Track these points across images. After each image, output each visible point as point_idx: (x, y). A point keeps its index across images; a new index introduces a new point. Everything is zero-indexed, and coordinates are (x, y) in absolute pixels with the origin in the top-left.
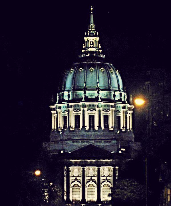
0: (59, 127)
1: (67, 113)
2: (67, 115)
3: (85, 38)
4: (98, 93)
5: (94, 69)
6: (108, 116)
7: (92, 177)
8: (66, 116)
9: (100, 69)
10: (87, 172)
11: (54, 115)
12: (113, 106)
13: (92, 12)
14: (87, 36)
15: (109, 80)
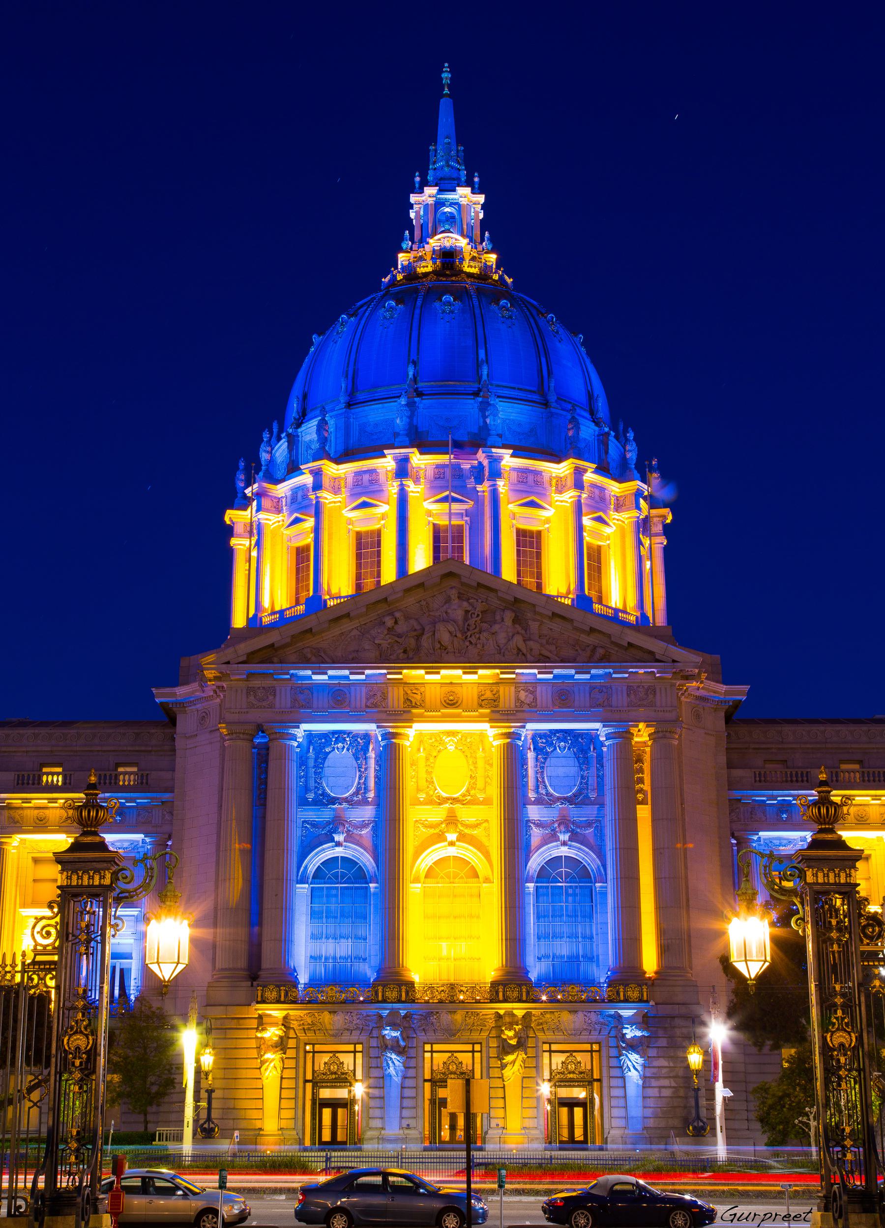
0: (266, 603)
1: (310, 522)
2: (309, 540)
3: (413, 198)
4: (485, 407)
5: (458, 304)
6: (539, 533)
7: (457, 806)
8: (307, 548)
9: (494, 307)
10: (423, 775)
11: (240, 544)
12: (570, 481)
13: (446, 91)
14: (425, 183)
15: (543, 360)
